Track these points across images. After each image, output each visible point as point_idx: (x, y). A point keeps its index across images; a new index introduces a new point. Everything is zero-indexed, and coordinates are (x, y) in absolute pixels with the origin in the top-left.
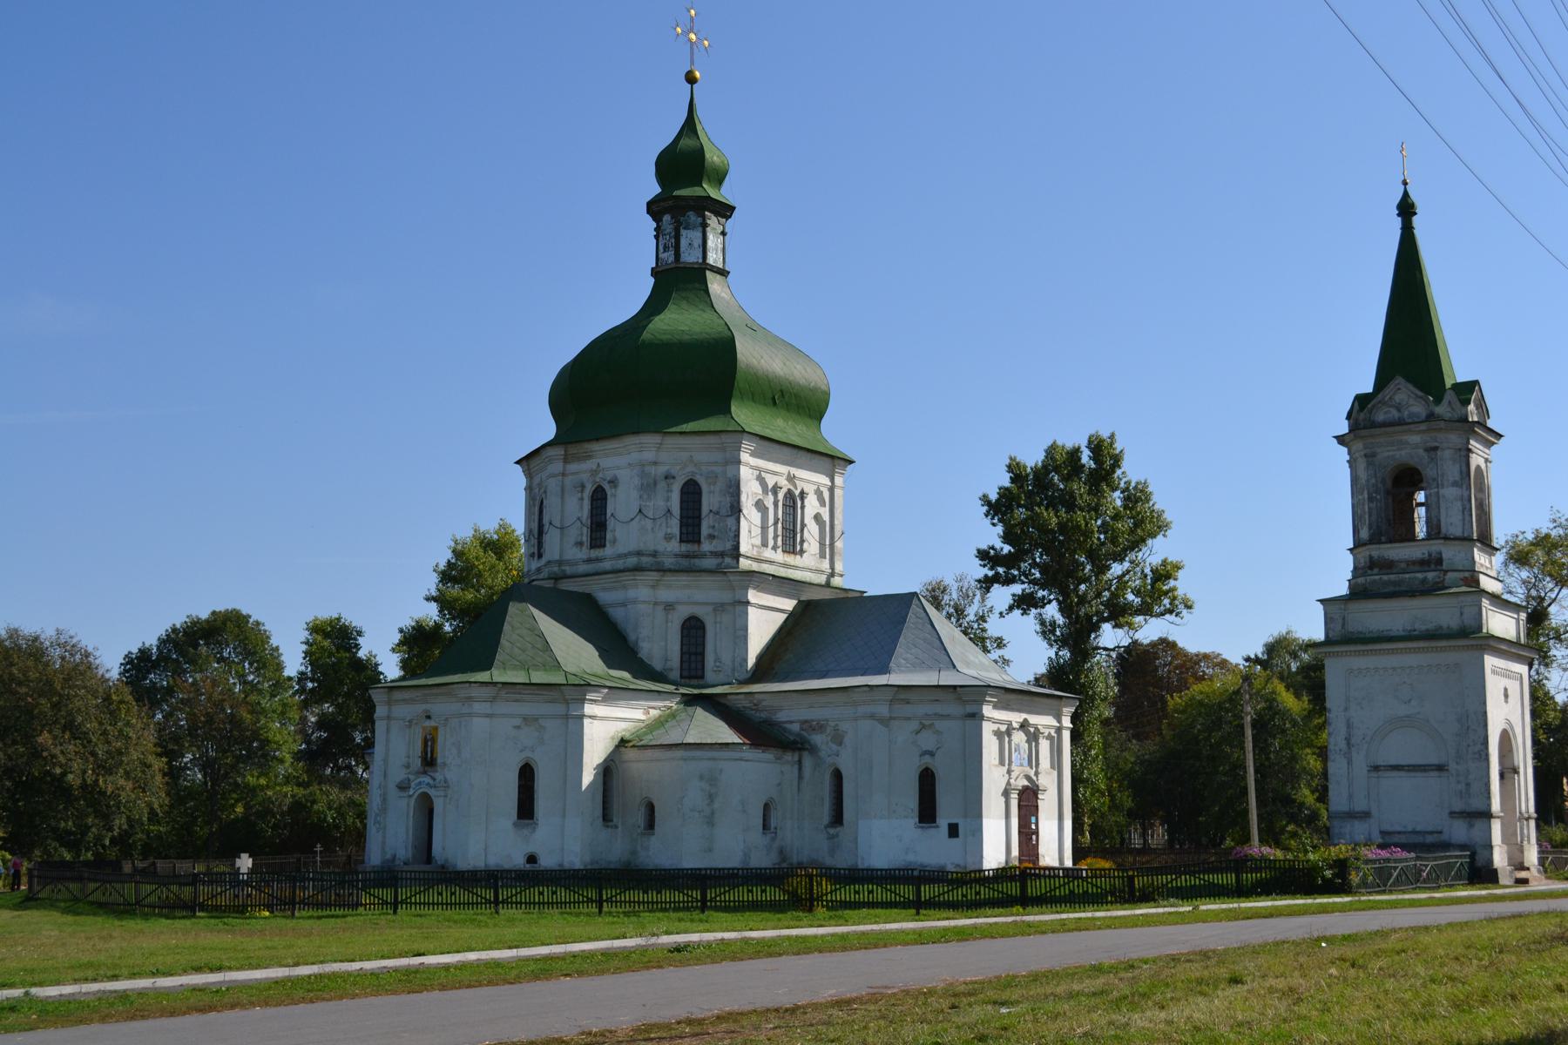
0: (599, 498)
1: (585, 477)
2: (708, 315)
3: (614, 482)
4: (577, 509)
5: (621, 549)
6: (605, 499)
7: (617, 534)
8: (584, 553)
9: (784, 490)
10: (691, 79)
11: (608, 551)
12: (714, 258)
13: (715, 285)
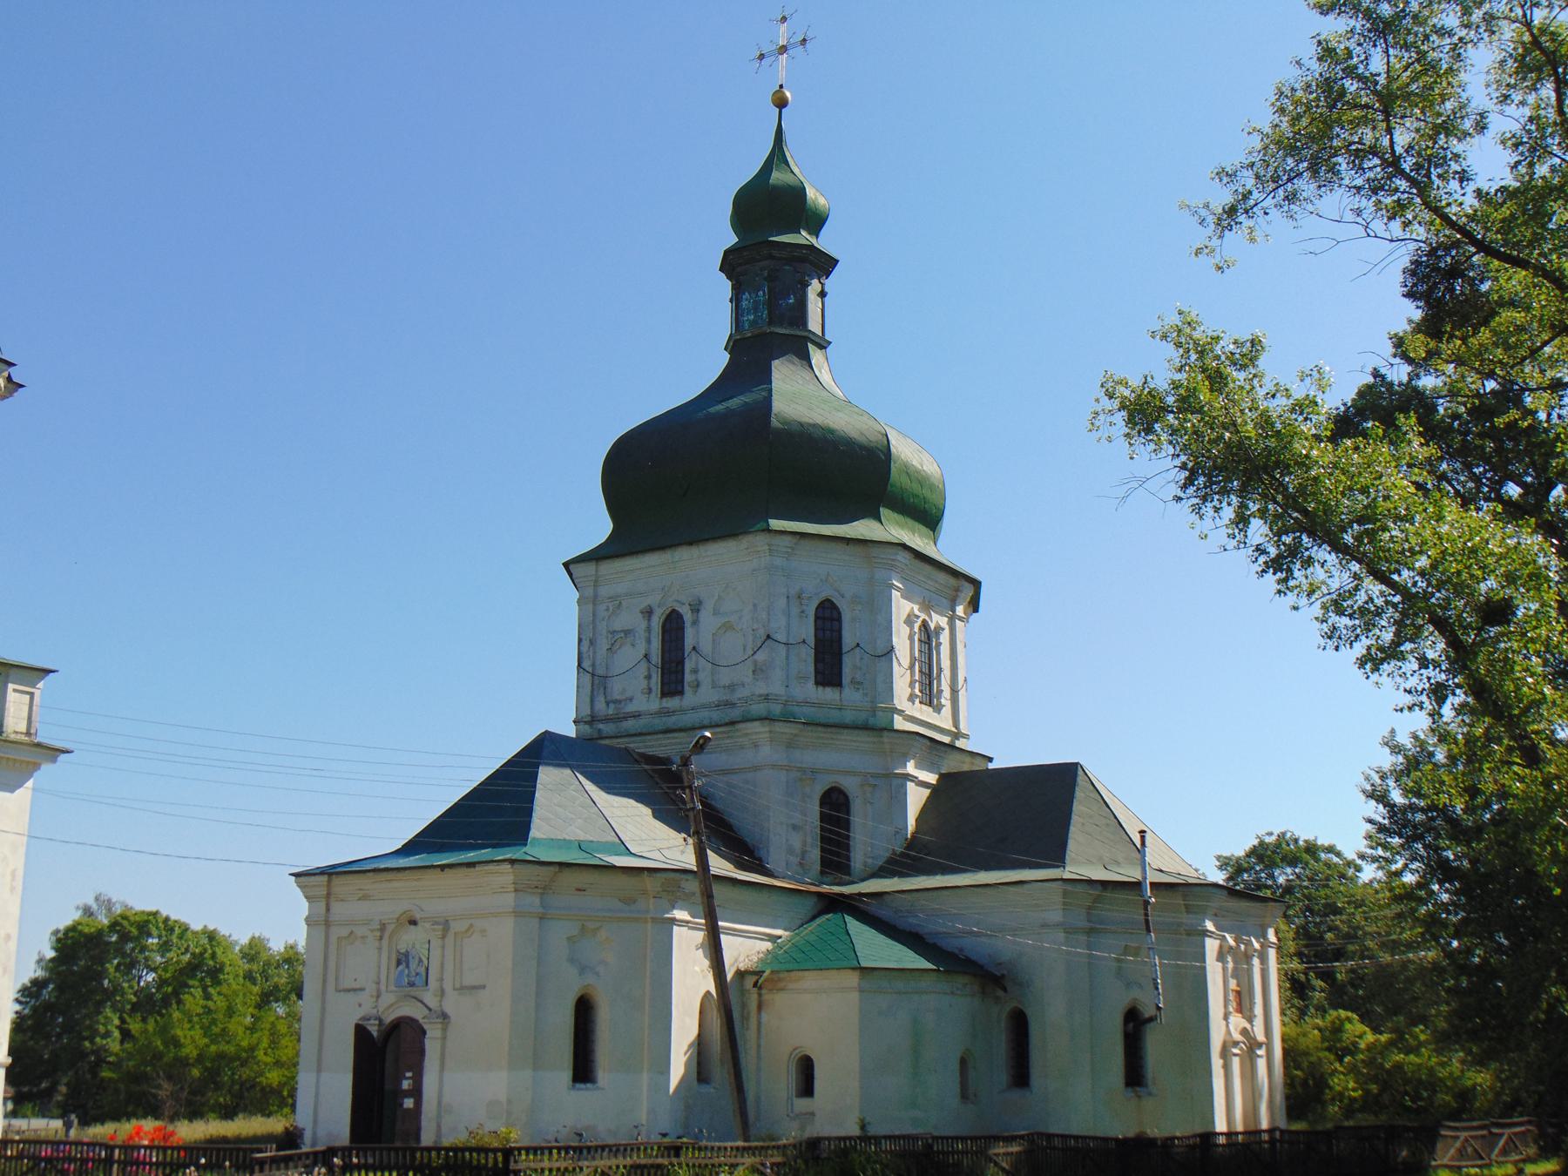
0: (673, 627)
1: (654, 600)
2: (812, 387)
3: (696, 608)
4: (645, 645)
5: (707, 695)
6: (681, 629)
7: (703, 676)
8: (655, 704)
9: (919, 622)
10: (781, 103)
11: (689, 698)
12: (814, 325)
13: (816, 356)
